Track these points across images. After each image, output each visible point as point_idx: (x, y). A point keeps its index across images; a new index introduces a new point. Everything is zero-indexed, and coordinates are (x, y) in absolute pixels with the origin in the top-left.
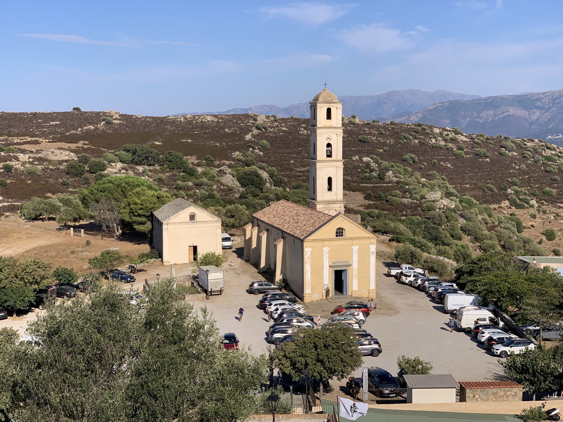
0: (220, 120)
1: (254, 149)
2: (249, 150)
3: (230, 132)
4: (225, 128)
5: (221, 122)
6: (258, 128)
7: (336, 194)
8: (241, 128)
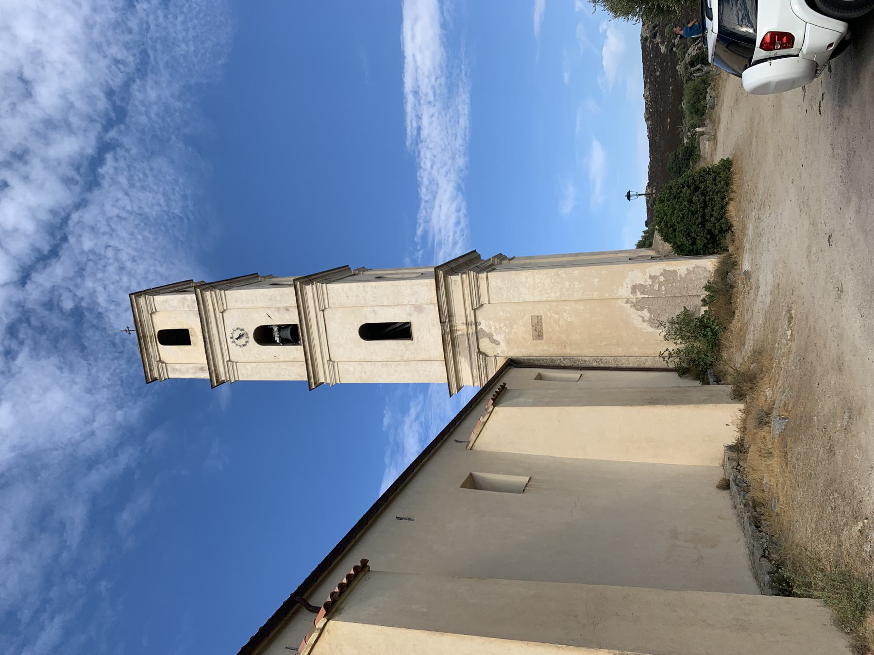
0: (648, 80)
1: (674, 45)
2: (675, 52)
3: (659, 70)
4: (655, 75)
5: (650, 79)
6: (655, 36)
7: (419, 309)
8: (656, 56)
